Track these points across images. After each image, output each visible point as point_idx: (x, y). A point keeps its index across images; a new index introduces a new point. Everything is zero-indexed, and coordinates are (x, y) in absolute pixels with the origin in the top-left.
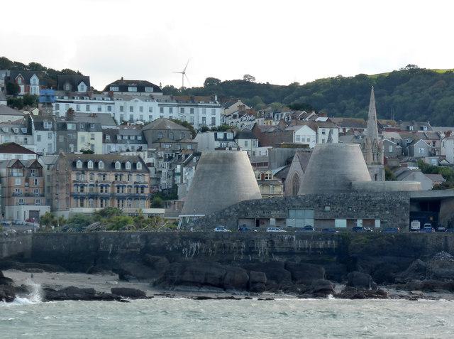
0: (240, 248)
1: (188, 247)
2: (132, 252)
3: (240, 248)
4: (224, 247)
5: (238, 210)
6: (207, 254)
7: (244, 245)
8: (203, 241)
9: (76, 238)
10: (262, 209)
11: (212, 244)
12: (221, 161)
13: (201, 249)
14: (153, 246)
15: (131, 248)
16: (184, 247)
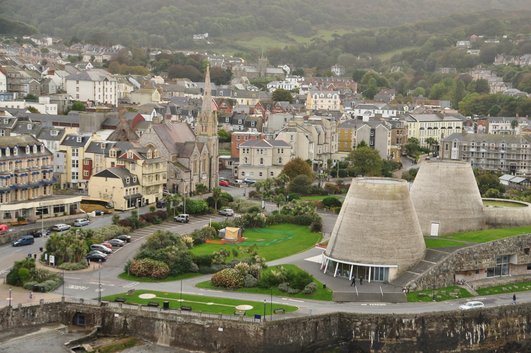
0: (522, 325)
1: (471, 330)
2: (406, 342)
3: (522, 325)
4: (508, 326)
5: (454, 263)
6: (493, 337)
7: (525, 322)
8: (488, 322)
9: (317, 324)
10: (475, 259)
11: (497, 324)
12: (399, 195)
13: (486, 332)
14: (431, 333)
15: (403, 337)
16: (466, 330)
